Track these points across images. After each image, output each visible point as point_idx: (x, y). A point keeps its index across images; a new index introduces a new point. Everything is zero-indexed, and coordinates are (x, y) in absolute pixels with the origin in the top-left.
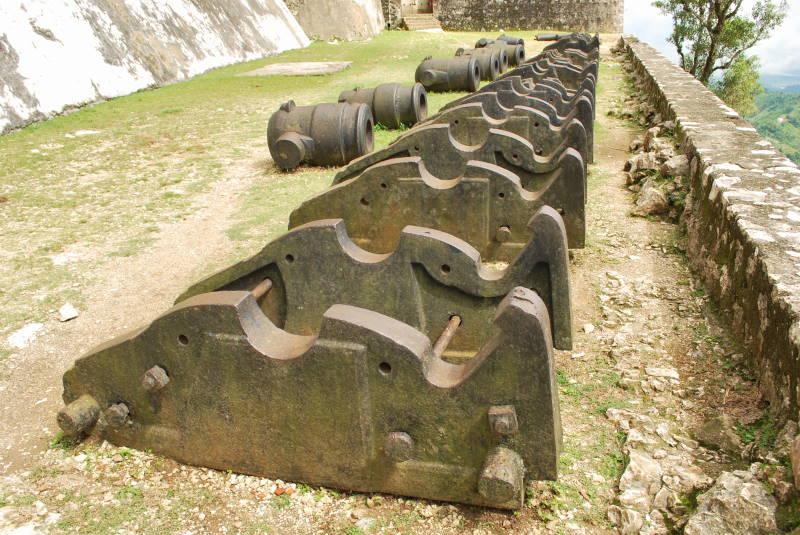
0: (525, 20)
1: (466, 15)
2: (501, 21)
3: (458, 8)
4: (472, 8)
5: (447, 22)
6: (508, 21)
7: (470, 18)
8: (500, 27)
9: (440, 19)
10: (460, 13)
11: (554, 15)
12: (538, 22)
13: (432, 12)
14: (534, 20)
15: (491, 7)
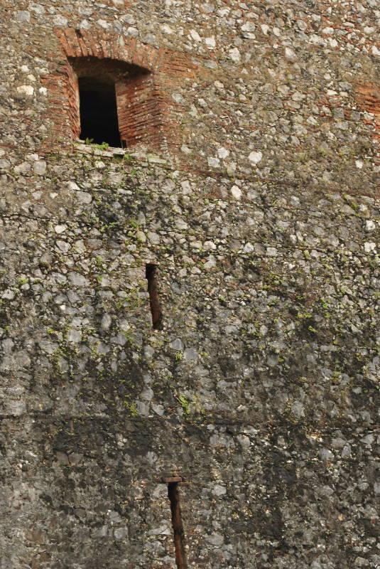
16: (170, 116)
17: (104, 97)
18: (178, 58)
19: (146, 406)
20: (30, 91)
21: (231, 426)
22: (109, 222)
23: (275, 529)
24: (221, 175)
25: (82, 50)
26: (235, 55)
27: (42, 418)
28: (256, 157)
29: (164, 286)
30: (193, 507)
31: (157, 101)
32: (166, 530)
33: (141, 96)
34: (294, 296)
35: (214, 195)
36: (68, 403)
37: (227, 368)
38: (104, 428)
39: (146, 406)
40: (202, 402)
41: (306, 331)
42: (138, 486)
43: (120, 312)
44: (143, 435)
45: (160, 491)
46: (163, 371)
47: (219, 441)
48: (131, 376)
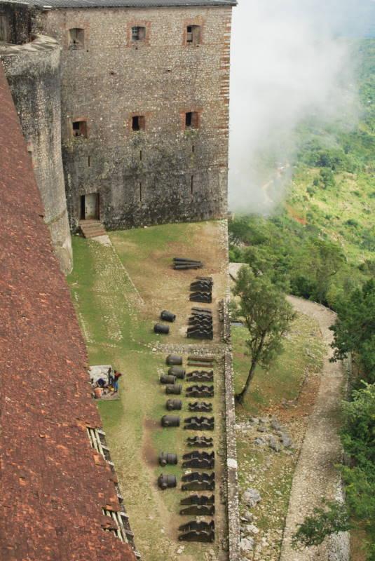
0: (160, 219)
1: (122, 219)
2: (145, 220)
3: (116, 216)
4: (126, 214)
5: (109, 225)
6: (150, 220)
7: (124, 221)
8: (145, 224)
9: (104, 223)
10: (117, 218)
11: (180, 213)
12: (169, 218)
13: (99, 219)
14: (167, 217)
15: (138, 212)
16: (147, 124)
17: (137, 123)
18: (149, 113)
19: (138, 172)
20: (125, 125)
21: (149, 173)
22: (135, 145)
23: (154, 187)
24: (154, 133)
25: (134, 115)
26: (159, 109)
27: (124, 176)
28: (160, 128)
29: (143, 153)
30: (142, 186)
31: (144, 122)
32: (139, 189)
33: (142, 120)
34: (162, 151)
35: (151, 137)
36: (127, 174)
37: (150, 165)
38: (131, 176)
39: (138, 172)
40: (147, 170)
41: (163, 157)
42: (136, 184)
43: (135, 159)
44: (137, 176)
45: (139, 184)
46: (141, 167)
47: (148, 176)
48: (136, 169)
